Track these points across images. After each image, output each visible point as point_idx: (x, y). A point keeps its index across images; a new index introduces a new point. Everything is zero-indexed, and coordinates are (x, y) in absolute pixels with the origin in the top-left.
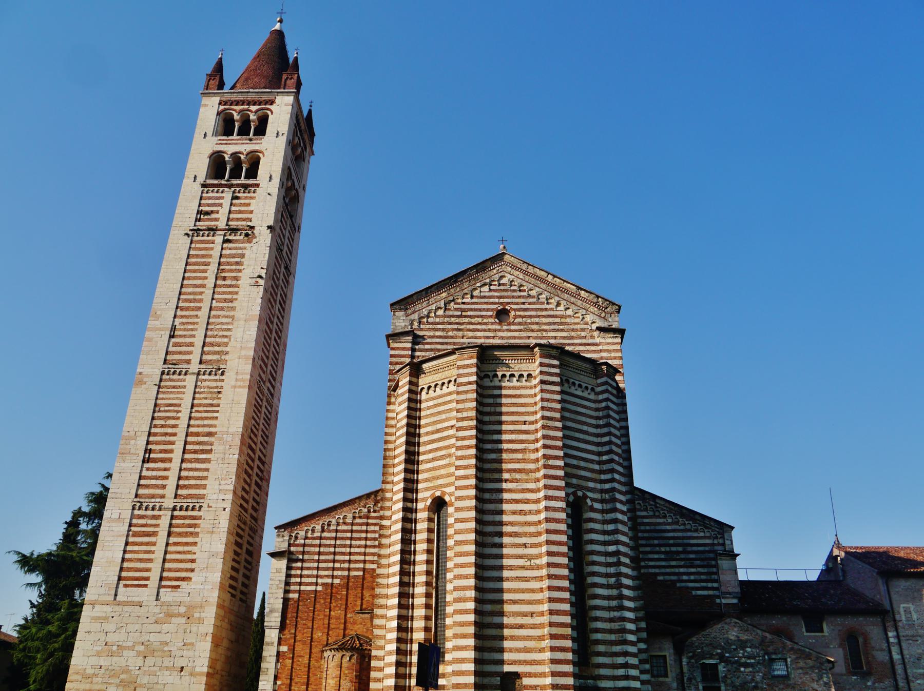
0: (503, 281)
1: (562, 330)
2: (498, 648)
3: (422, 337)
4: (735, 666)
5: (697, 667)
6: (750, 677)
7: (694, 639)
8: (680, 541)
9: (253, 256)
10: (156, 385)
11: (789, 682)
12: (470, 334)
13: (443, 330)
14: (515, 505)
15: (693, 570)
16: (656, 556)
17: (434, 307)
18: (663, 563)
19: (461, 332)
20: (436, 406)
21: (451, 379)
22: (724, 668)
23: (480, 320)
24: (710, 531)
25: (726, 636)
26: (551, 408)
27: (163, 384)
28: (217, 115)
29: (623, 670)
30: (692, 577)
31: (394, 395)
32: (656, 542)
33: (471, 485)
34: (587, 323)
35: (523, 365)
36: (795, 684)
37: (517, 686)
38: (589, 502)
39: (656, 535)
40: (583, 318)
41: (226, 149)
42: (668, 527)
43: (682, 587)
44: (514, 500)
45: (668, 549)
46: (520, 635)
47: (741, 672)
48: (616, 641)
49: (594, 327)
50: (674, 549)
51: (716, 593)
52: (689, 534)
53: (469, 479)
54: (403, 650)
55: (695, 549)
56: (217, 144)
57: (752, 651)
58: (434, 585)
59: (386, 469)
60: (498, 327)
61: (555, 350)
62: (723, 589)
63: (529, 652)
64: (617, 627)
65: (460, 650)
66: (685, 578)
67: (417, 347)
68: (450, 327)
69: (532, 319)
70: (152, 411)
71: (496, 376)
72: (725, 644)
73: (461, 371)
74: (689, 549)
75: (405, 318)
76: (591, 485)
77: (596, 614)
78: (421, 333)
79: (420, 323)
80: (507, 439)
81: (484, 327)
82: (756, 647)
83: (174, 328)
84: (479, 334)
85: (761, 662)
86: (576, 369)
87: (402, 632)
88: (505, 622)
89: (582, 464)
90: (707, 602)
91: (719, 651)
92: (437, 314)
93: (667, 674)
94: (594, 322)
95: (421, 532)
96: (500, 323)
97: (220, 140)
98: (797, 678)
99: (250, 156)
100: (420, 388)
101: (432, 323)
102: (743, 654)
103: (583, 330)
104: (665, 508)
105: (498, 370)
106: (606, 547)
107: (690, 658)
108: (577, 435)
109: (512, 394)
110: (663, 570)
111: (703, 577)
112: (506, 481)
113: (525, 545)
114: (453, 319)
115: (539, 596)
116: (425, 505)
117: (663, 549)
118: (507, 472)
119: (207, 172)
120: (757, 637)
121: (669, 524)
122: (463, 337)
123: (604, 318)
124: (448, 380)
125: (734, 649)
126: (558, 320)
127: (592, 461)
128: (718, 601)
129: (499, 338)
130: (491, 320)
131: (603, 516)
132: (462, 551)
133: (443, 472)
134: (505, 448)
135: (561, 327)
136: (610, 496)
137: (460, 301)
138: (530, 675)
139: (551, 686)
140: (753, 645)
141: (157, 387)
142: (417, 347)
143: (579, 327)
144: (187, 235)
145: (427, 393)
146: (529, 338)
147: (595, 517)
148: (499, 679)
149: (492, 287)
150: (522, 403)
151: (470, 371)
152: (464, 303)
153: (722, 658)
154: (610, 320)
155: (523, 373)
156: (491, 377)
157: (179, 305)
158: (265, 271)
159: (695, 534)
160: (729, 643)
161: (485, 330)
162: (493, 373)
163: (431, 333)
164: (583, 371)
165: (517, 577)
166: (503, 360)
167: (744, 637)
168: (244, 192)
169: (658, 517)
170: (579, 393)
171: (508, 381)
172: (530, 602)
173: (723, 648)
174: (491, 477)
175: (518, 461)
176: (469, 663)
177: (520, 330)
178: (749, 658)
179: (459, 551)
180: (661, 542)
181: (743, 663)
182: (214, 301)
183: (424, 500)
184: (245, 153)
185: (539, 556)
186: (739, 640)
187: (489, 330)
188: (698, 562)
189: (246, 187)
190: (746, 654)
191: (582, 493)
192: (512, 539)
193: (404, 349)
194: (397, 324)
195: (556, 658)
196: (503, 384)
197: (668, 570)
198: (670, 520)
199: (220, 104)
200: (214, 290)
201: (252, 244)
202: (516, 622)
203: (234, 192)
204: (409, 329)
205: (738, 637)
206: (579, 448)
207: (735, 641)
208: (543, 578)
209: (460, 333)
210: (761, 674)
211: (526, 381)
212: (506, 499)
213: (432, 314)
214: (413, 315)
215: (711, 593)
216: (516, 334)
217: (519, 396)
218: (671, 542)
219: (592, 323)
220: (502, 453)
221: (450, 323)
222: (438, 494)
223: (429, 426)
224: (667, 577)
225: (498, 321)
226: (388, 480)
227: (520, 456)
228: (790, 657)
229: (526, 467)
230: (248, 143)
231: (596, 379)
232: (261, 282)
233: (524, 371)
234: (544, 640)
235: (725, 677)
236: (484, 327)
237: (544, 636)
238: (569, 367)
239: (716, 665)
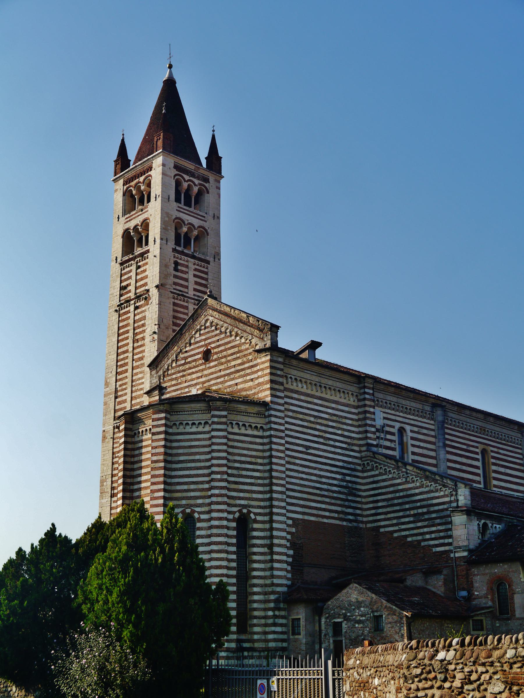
0: (208, 324)
4: (352, 623)
5: (330, 625)
6: (361, 632)
7: (330, 603)
8: (425, 503)
9: (150, 316)
10: (111, 438)
11: (384, 635)
15: (434, 529)
16: (407, 520)
17: (170, 361)
18: (412, 525)
19: (185, 378)
22: (346, 625)
24: (447, 489)
25: (349, 599)
26: (157, 453)
27: (116, 436)
28: (123, 196)
30: (433, 536)
32: (407, 506)
36: (386, 636)
38: (196, 515)
39: (407, 500)
41: (146, 216)
42: (417, 491)
43: (425, 546)
45: (416, 511)
47: (356, 628)
50: (420, 511)
51: (451, 548)
52: (432, 495)
55: (436, 508)
56: (125, 223)
57: (364, 610)
61: (162, 406)
62: (455, 544)
66: (428, 536)
68: (179, 375)
70: (111, 458)
72: (348, 605)
73: (155, 423)
74: (432, 509)
76: (200, 501)
82: (367, 607)
83: (116, 391)
85: (369, 619)
86: (191, 411)
89: (192, 487)
90: (444, 557)
91: (344, 611)
92: (173, 366)
93: (300, 632)
97: (126, 218)
98: (388, 631)
99: (144, 224)
102: (359, 613)
104: (413, 473)
107: (327, 618)
110: (412, 532)
111: (442, 534)
117: (412, 512)
119: (122, 251)
120: (368, 598)
121: (417, 488)
125: (353, 609)
127: (202, 483)
128: (452, 555)
137: (184, 350)
140: (365, 605)
141: (112, 439)
144: (116, 311)
146: (220, 371)
149: (202, 332)
152: (186, 352)
153: (346, 618)
157: (118, 371)
158: (157, 327)
159: (437, 494)
160: (351, 605)
161: (197, 372)
164: (198, 411)
167: (361, 599)
168: (142, 261)
169: (408, 482)
170: (194, 429)
173: (346, 609)
178: (362, 616)
180: (411, 505)
181: (358, 620)
182: (134, 362)
184: (140, 224)
186: (358, 602)
188: (438, 521)
189: (142, 255)
190: (360, 613)
191: (190, 510)
197: (415, 532)
198: (418, 484)
199: (124, 185)
200: (133, 352)
201: (149, 306)
203: (137, 263)
205: (357, 599)
206: (190, 475)
207: (355, 602)
210: (368, 629)
213: (170, 367)
215: (447, 548)
216: (213, 370)
218: (418, 504)
224: (415, 538)
228: (385, 614)
230: (141, 214)
232: (156, 336)
235: (346, 632)
238: (184, 411)
239: (341, 622)
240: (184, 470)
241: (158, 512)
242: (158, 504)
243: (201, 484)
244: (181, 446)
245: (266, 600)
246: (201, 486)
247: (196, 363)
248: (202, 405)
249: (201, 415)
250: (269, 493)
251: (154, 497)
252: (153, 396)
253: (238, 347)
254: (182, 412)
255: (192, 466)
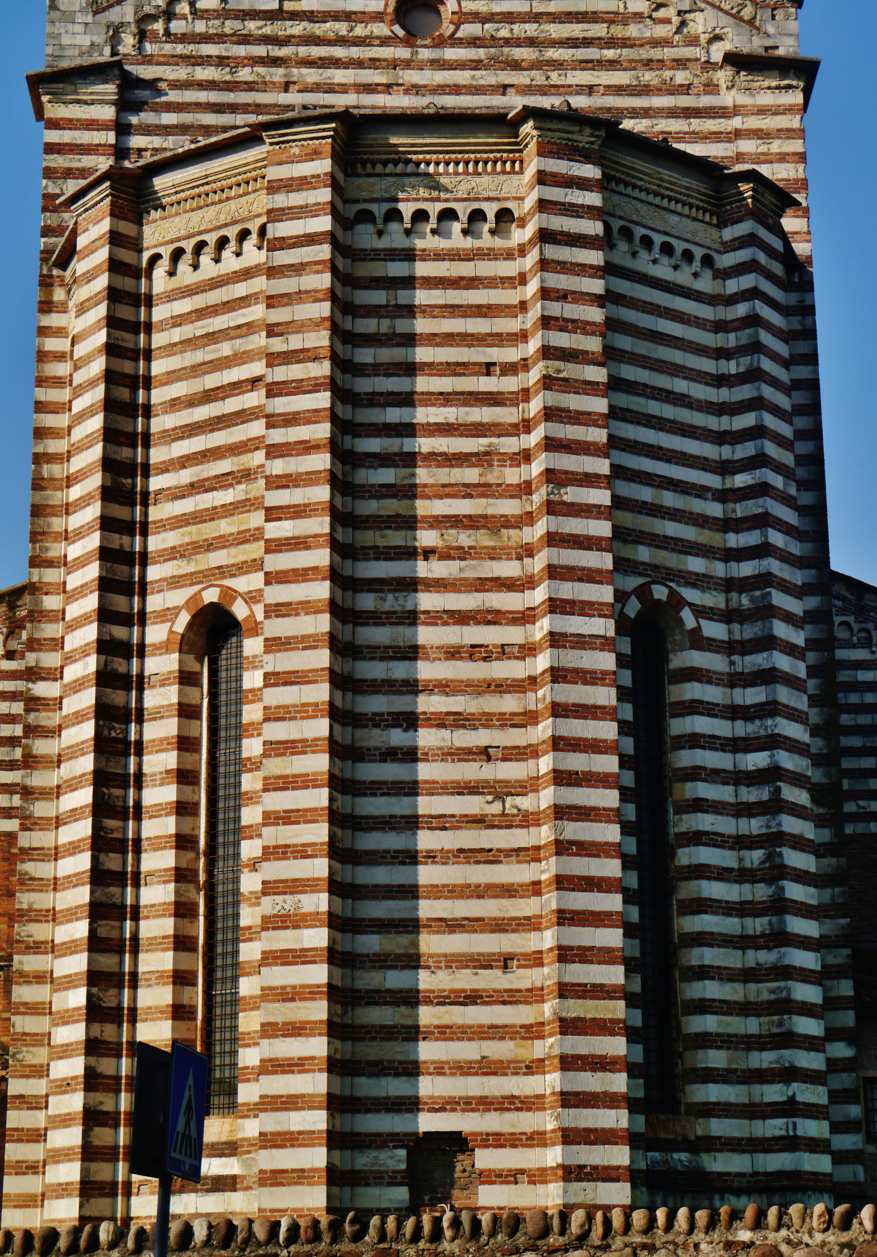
1: (613, 65)
2: (400, 1062)
3: (152, 84)
12: (312, 75)
13: (221, 61)
14: (457, 628)
19: (281, 71)
20: (201, 314)
21: (249, 225)
23: (342, 28)
26: (574, 321)
29: (780, 1122)
31: (62, 278)
33: (315, 569)
34: (693, 41)
35: (485, 180)
37: (457, 1175)
38: (688, 618)
40: (683, 24)
44: (451, 613)
46: (468, 1022)
48: (760, 1036)
49: (717, 52)
53: (308, 548)
54: (109, 1077)
58: (202, 877)
59: (41, 521)
60: (403, 53)
61: (588, 131)
63: (495, 1074)
64: (765, 996)
65: (284, 1072)
67: (134, 120)
68: (241, 51)
69: (515, 27)
71: (395, 215)
75: (89, 19)
76: (696, 564)
77: (701, 957)
78: (146, 72)
79: (142, 36)
80: (432, 420)
81: (355, 52)
84: (340, 76)
86: (656, 194)
87: (100, 1022)
88: (422, 986)
89: (669, 499)
94: (717, 38)
95: (158, 715)
96: (410, 40)
100: (146, 256)
101: (183, 38)
103: (681, 63)
105: (401, 195)
106: (739, 756)
108: (655, 408)
109: (446, 274)
112: (428, 553)
113: (485, 754)
114: (252, 26)
115: (527, 907)
116: (171, 632)
118: (431, 527)
122: (286, 87)
123: (751, 22)
124: (237, 229)
126: (599, 30)
127: (700, 491)
129: (407, 92)
130: (381, 29)
131: (732, 663)
132: (288, 772)
133: (225, 526)
134: (425, 450)
135: (610, 54)
136: (752, 600)
138: (497, 1140)
139: (560, 1172)
142: (134, 120)
143: (668, 53)
145: (172, 273)
146: (504, 89)
147: (705, 666)
148: (402, 1153)
150: (479, 306)
151: (311, 201)
154: (771, 30)
155: (485, 206)
156: (380, 220)
161: (359, 64)
162: (386, 206)
163: (181, 73)
164: (677, 201)
165: (461, 851)
166: (418, 164)
170: (663, 271)
171: (434, 232)
172: (499, 926)
174: (381, 543)
175: (467, 491)
176: (310, 1108)
177: (476, 65)
179: (278, 772)
183: (168, 615)
185: (529, 786)
187: (374, 63)
191: (666, 591)
192: (445, 733)
193: (90, 125)
194: (66, 40)
195: (579, 1089)
196: (419, 244)
202: (458, 985)
204: (106, 56)
206: (660, 448)
208: (542, 853)
209: (278, 74)
211: (492, 232)
212: (427, 612)
214: (117, 8)
216: (462, 77)
217: (472, 283)
219: (710, 41)
220: (415, 466)
221: (245, 39)
222: (211, 596)
223: (180, 379)
225: (401, 33)
226: (52, 554)
227: (471, 475)
229: (490, 511)
231: (721, 225)
233: (488, 199)
234: (542, 1037)
236: (355, 52)
237: (542, 1024)
238: (634, 187)
240: (639, 423)
241: (590, 570)
242: (589, 538)
243: (697, 496)
244: (625, 323)
245: (749, 1003)
246: (698, 506)
247: (352, 29)
248: (694, 184)
249: (689, 221)
250: (812, 595)
251: (564, 503)
252: (78, 102)
253: (611, 22)
254: (626, 185)
255: (665, 415)
